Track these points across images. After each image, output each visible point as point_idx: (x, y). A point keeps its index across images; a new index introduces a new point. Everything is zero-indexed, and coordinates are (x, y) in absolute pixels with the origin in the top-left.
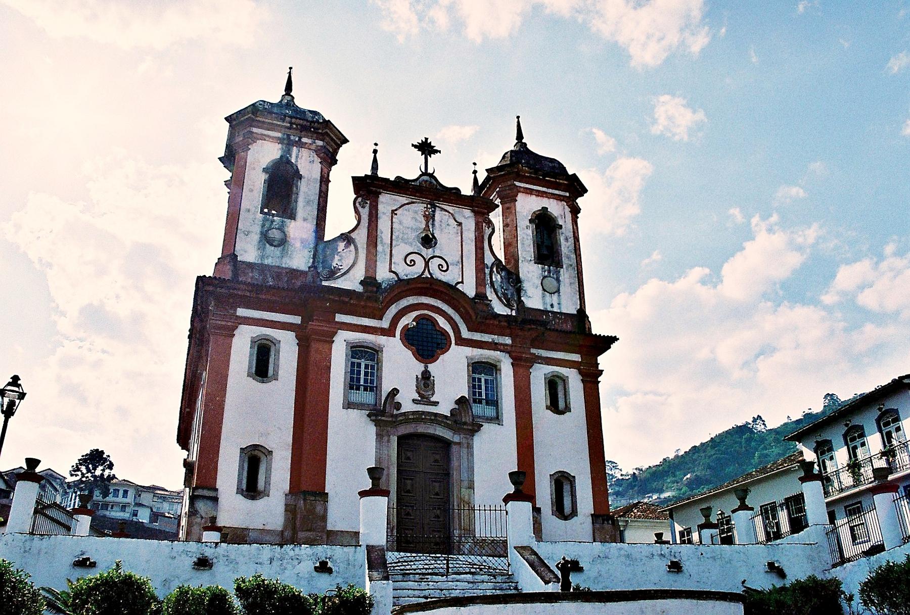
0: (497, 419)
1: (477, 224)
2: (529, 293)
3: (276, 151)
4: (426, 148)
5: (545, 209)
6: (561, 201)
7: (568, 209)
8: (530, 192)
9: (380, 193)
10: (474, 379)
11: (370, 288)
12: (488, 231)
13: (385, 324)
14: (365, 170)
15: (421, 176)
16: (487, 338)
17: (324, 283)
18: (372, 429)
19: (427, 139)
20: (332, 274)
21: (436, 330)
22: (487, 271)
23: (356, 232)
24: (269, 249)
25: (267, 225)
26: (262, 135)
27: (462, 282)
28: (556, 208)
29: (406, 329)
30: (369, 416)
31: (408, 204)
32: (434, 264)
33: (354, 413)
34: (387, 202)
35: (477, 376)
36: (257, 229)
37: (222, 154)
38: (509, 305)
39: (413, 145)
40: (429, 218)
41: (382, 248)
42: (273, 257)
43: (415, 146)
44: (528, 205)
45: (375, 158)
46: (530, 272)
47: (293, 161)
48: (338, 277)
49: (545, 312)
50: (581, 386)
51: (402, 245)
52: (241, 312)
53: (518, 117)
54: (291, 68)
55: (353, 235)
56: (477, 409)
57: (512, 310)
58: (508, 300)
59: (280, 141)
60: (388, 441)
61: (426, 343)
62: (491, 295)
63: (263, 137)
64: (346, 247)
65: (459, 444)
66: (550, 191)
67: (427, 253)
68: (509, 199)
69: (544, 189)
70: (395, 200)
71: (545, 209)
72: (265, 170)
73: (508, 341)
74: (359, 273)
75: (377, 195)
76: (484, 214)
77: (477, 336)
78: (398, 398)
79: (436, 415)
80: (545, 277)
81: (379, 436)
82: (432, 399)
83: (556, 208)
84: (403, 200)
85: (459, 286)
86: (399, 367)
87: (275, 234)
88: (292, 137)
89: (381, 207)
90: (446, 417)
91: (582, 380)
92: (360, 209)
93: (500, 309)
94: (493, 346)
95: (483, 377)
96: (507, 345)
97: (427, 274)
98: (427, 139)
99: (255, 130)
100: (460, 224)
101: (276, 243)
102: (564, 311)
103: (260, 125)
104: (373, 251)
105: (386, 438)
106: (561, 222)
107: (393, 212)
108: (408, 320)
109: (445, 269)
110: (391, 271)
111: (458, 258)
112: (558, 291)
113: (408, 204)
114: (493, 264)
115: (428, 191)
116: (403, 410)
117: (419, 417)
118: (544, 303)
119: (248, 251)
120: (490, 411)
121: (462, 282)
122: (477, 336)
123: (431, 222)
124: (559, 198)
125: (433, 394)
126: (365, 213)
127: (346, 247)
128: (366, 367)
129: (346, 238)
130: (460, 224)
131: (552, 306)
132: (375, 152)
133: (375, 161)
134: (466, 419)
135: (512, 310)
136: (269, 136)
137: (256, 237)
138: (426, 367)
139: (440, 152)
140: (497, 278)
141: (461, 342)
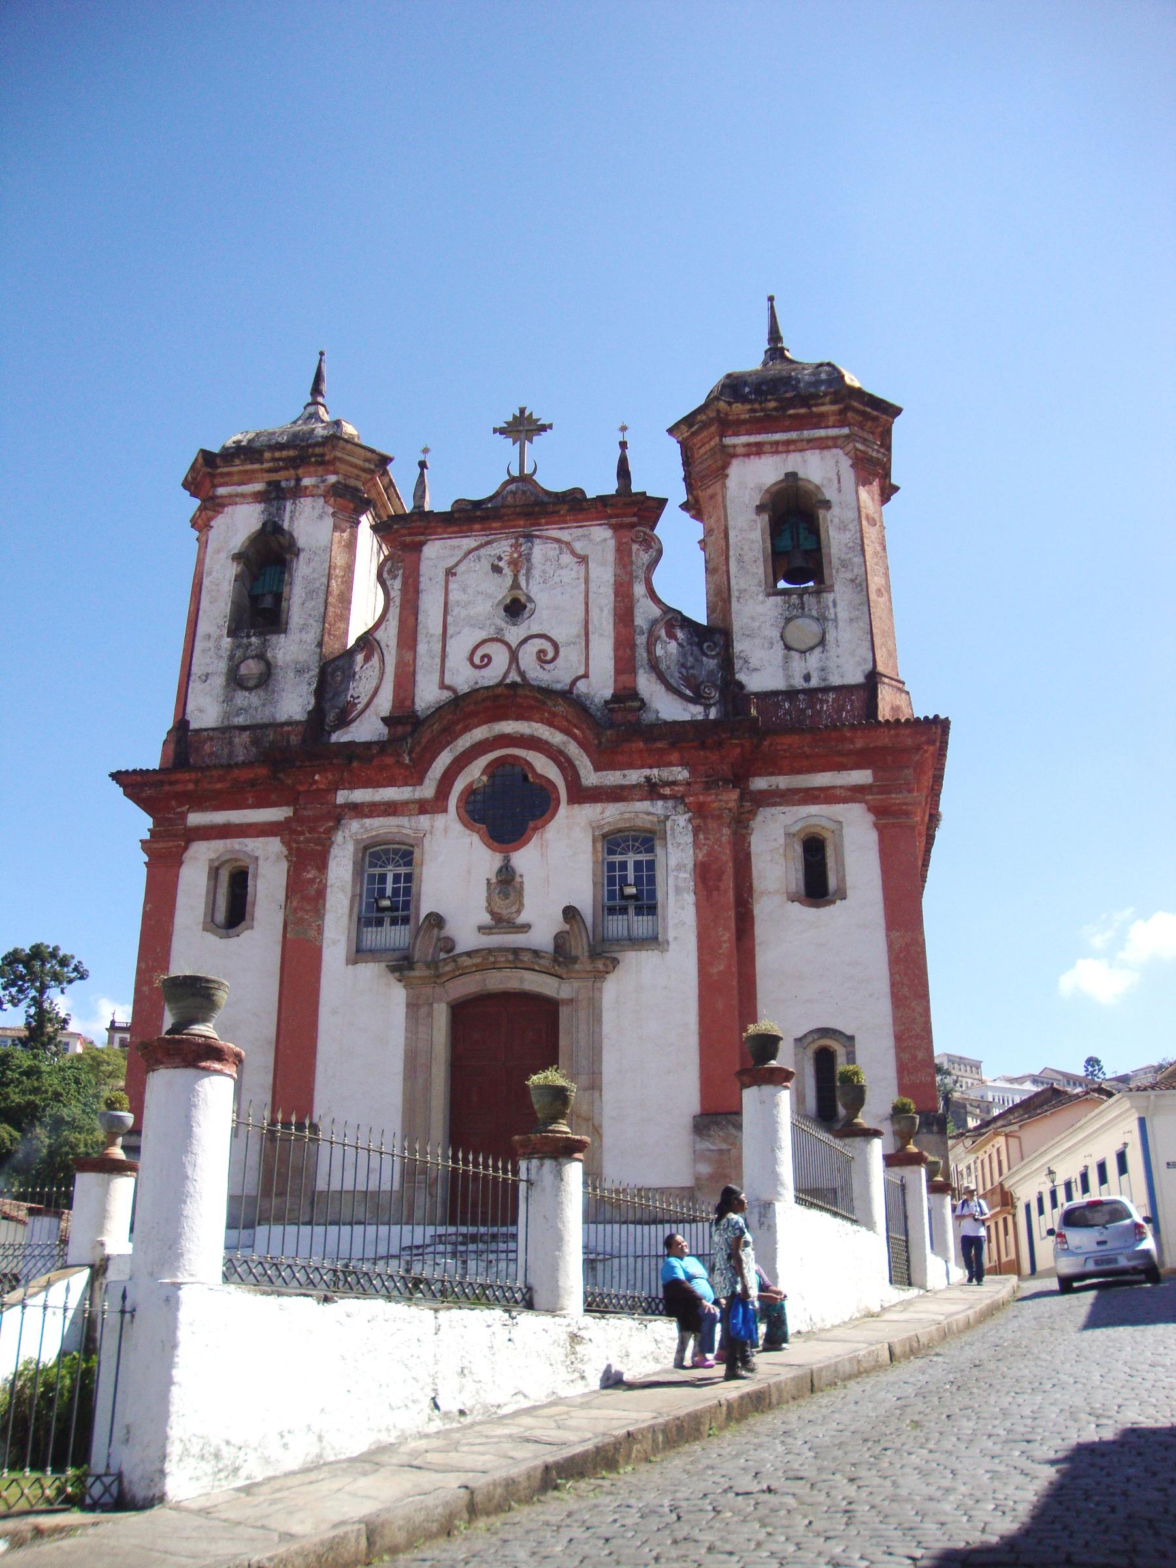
0: (653, 941)
1: (619, 550)
2: (754, 662)
3: (256, 515)
4: (523, 428)
5: (792, 476)
6: (828, 448)
7: (846, 463)
8: (757, 450)
9: (422, 544)
10: (611, 866)
11: (400, 730)
12: (642, 557)
13: (428, 790)
15: (507, 483)
16: (635, 776)
17: (335, 738)
18: (398, 995)
19: (522, 411)
20: (344, 720)
22: (641, 640)
23: (383, 627)
24: (241, 698)
25: (239, 653)
26: (231, 496)
27: (586, 676)
28: (822, 469)
29: (470, 792)
30: (393, 969)
31: (477, 549)
33: (370, 971)
34: (436, 553)
35: (617, 858)
36: (222, 666)
38: (697, 698)
39: (495, 431)
40: (520, 563)
41: (427, 649)
42: (251, 706)
43: (502, 431)
44: (752, 477)
45: (422, 475)
46: (757, 615)
47: (286, 526)
48: (353, 721)
49: (791, 694)
50: (873, 837)
51: (466, 630)
52: (196, 819)
53: (771, 299)
54: (322, 354)
55: (379, 635)
56: (617, 925)
57: (707, 707)
58: (696, 689)
59: (259, 497)
60: (430, 1014)
61: (509, 811)
62: (646, 684)
63: (233, 500)
64: (367, 659)
65: (570, 1001)
66: (806, 434)
67: (514, 634)
69: (793, 435)
70: (453, 548)
71: (792, 476)
72: (237, 557)
73: (681, 774)
74: (384, 703)
75: (418, 547)
76: (632, 526)
77: (612, 778)
78: (444, 933)
79: (516, 951)
80: (788, 620)
81: (413, 1007)
82: (522, 919)
83: (822, 469)
84: (468, 543)
85: (581, 686)
86: (454, 870)
87: (251, 668)
88: (283, 484)
89: (425, 568)
90: (536, 953)
91: (875, 825)
92: (389, 583)
93: (668, 708)
94: (652, 790)
95: (631, 859)
96: (674, 783)
97: (514, 677)
98: (522, 411)
99: (221, 491)
100: (583, 560)
101: (251, 684)
102: (836, 681)
103: (226, 479)
104: (408, 656)
105: (423, 1011)
106: (829, 494)
107: (450, 573)
108: (475, 772)
109: (550, 655)
111: (576, 629)
112: (822, 642)
113: (477, 549)
114: (654, 623)
115: (522, 510)
116: (460, 949)
117: (486, 959)
118: (788, 677)
119: (206, 712)
120: (640, 925)
121: (586, 676)
122: (612, 778)
123: (523, 571)
124: (822, 445)
125: (519, 912)
126: (396, 585)
127: (367, 659)
128: (397, 878)
129: (367, 642)
130: (583, 560)
131: (807, 678)
132: (423, 465)
134: (589, 948)
135: (707, 707)
136: (243, 496)
137: (219, 681)
138: (507, 860)
139: (550, 426)
140: (669, 650)
141: (580, 794)
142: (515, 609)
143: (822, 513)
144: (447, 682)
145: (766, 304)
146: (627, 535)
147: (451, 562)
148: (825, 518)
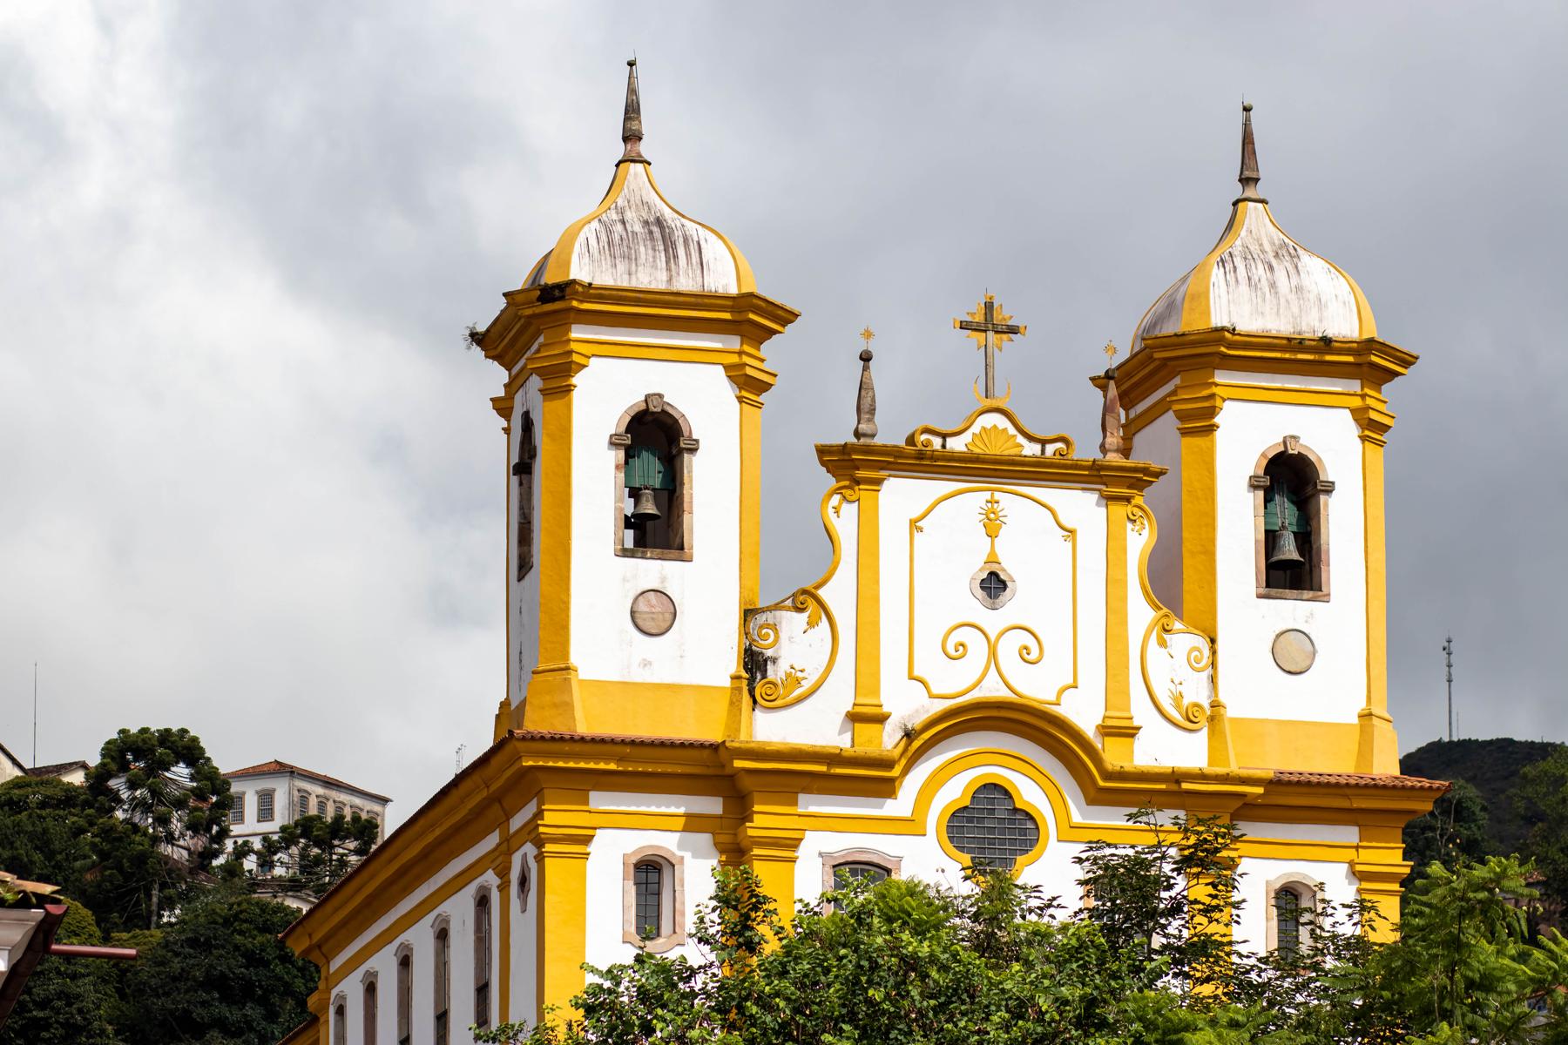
9: (879, 482)
14: (843, 435)
21: (1016, 810)
32: (1008, 649)
37: (482, 328)
48: (800, 700)
53: (1247, 109)
54: (631, 64)
55: (821, 593)
67: (993, 620)
68: (1200, 422)
107: (915, 525)
108: (955, 791)
109: (1034, 655)
110: (912, 678)
127: (812, 624)
132: (866, 358)
133: (864, 387)
142: (994, 585)
143: (1322, 498)
144: (916, 673)
145: (1240, 116)
146: (1120, 510)
147: (916, 514)
148: (1326, 505)
